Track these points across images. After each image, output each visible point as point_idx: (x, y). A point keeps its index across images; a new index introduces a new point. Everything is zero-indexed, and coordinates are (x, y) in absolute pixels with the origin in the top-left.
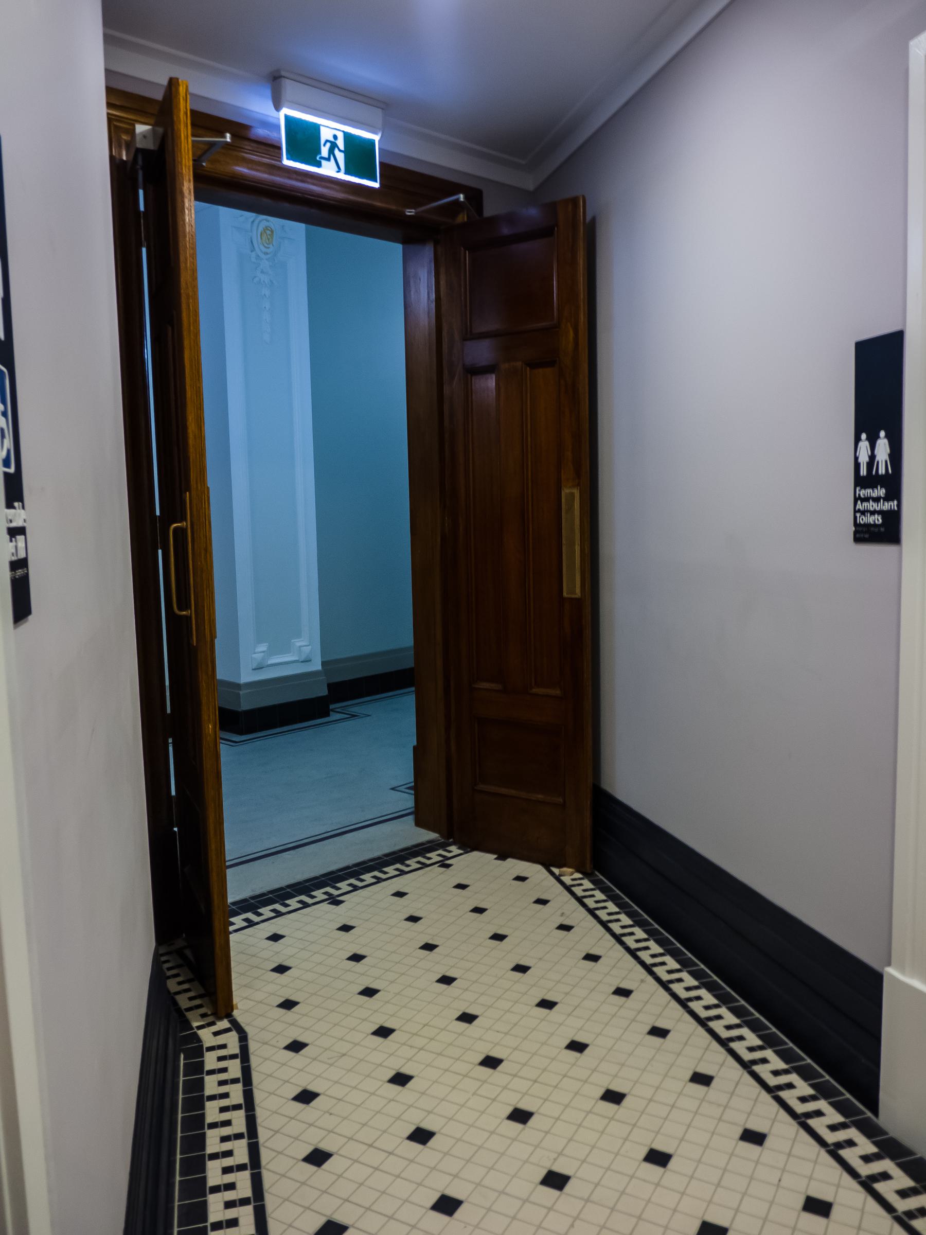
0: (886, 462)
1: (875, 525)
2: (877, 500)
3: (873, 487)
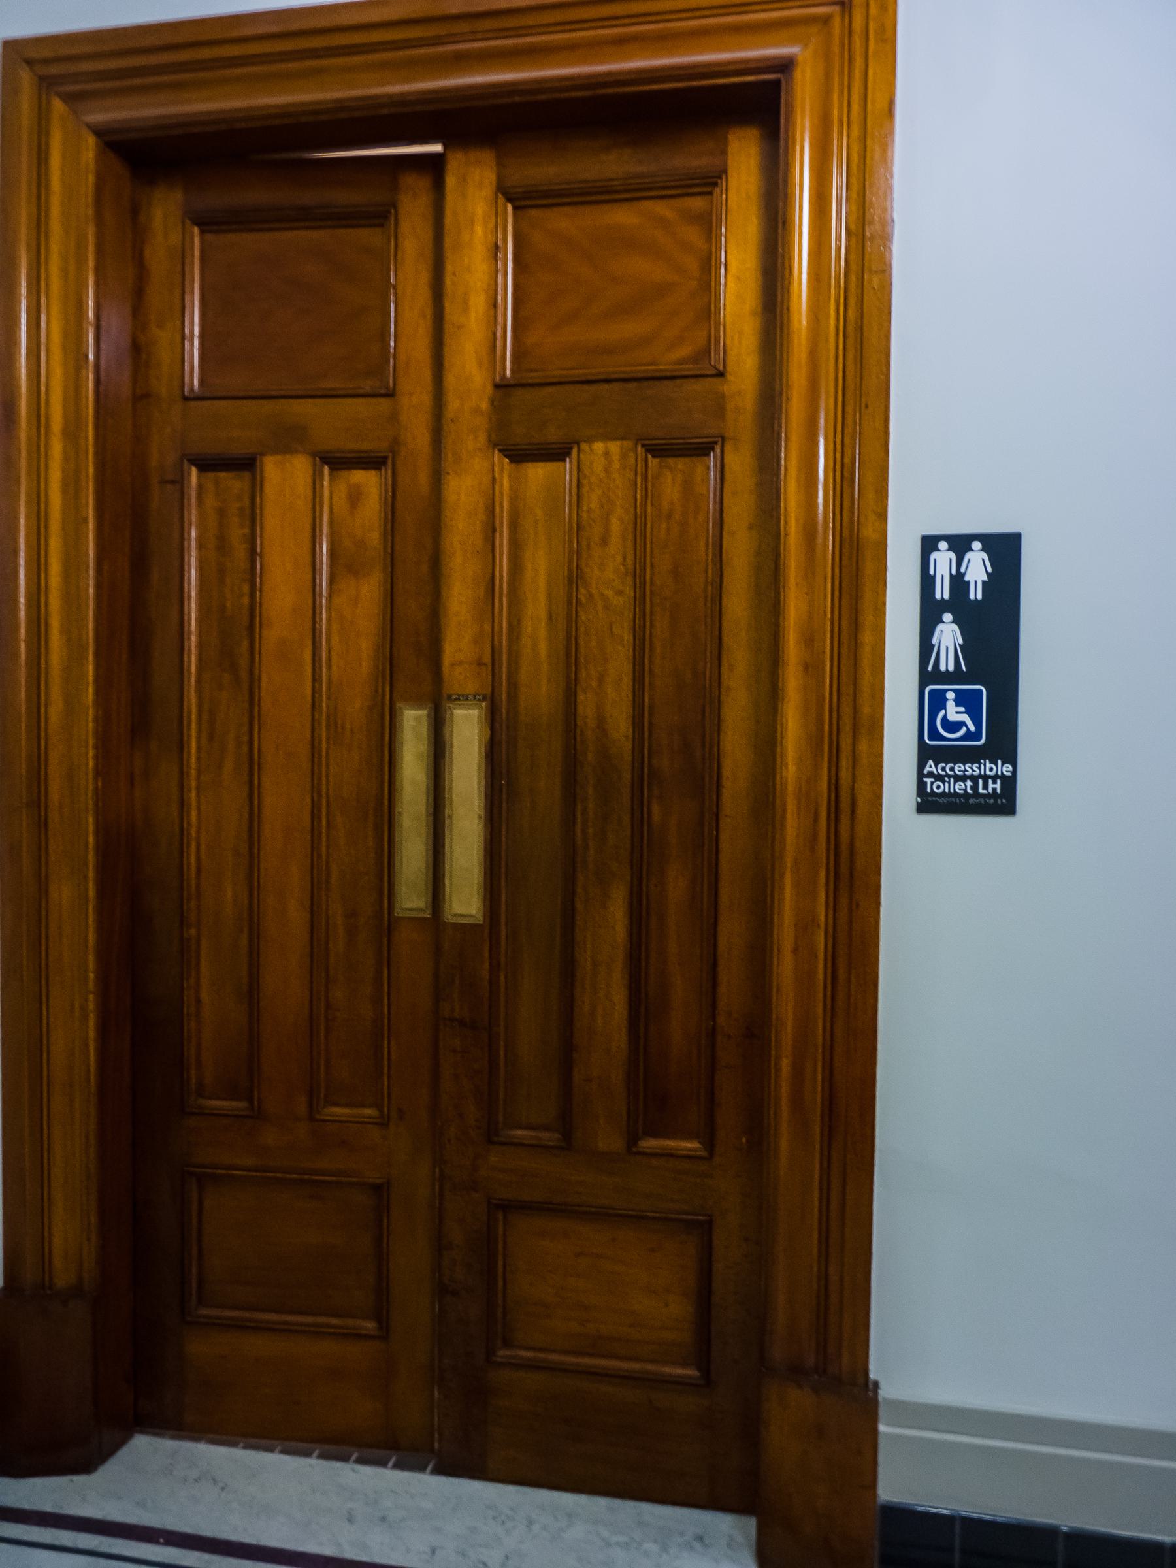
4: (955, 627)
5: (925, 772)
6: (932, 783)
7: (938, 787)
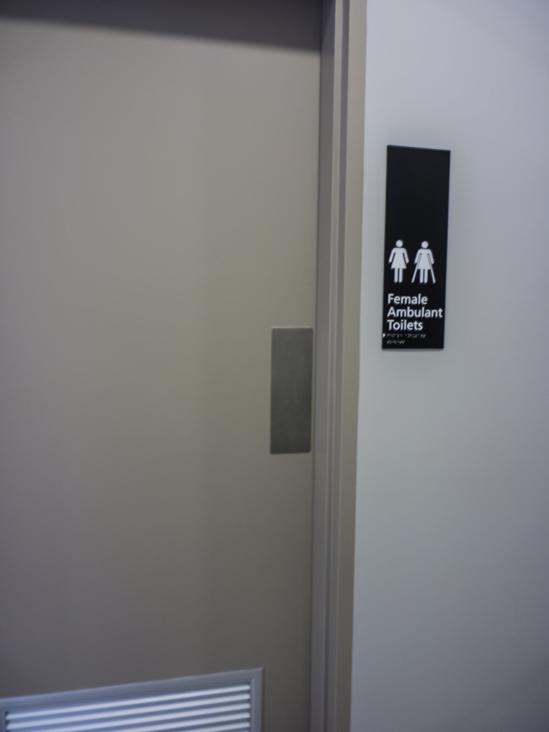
0: (429, 272)
1: (413, 332)
2: (417, 307)
3: (412, 294)
5: (388, 315)
6: (393, 323)
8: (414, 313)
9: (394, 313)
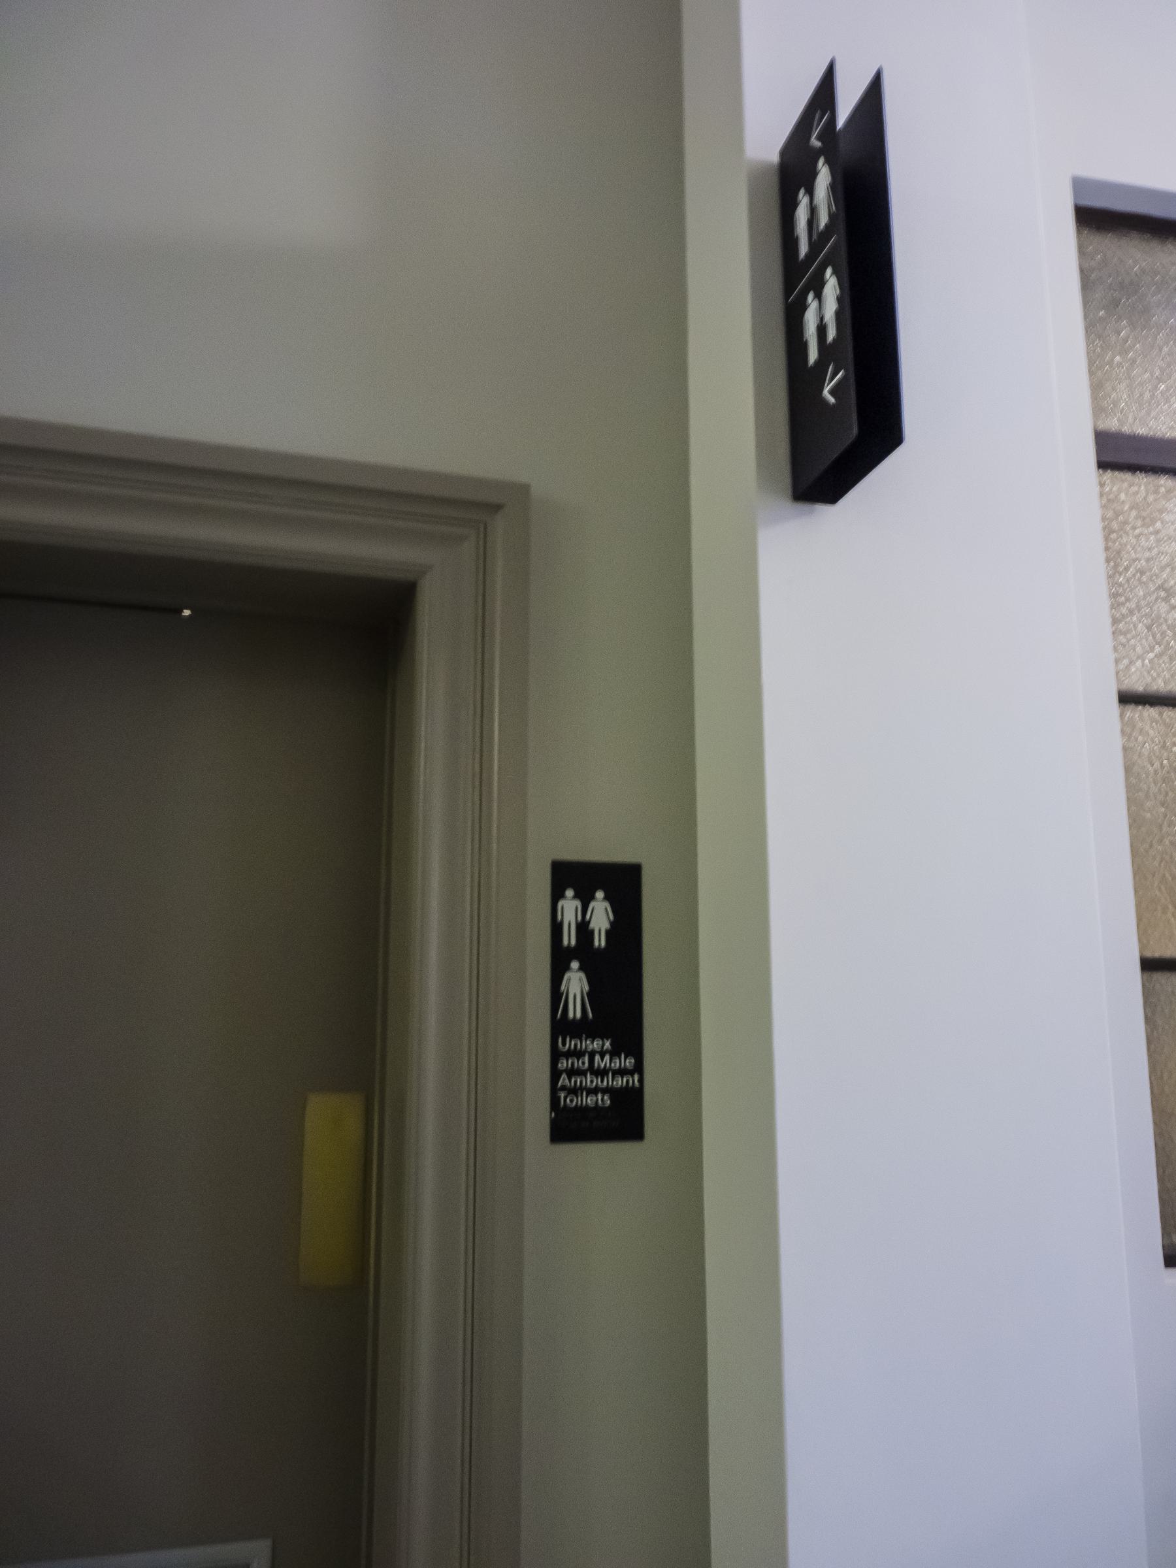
4: (582, 975)
6: (565, 1098)
7: (571, 1101)
8: (597, 1082)
9: (567, 1081)
